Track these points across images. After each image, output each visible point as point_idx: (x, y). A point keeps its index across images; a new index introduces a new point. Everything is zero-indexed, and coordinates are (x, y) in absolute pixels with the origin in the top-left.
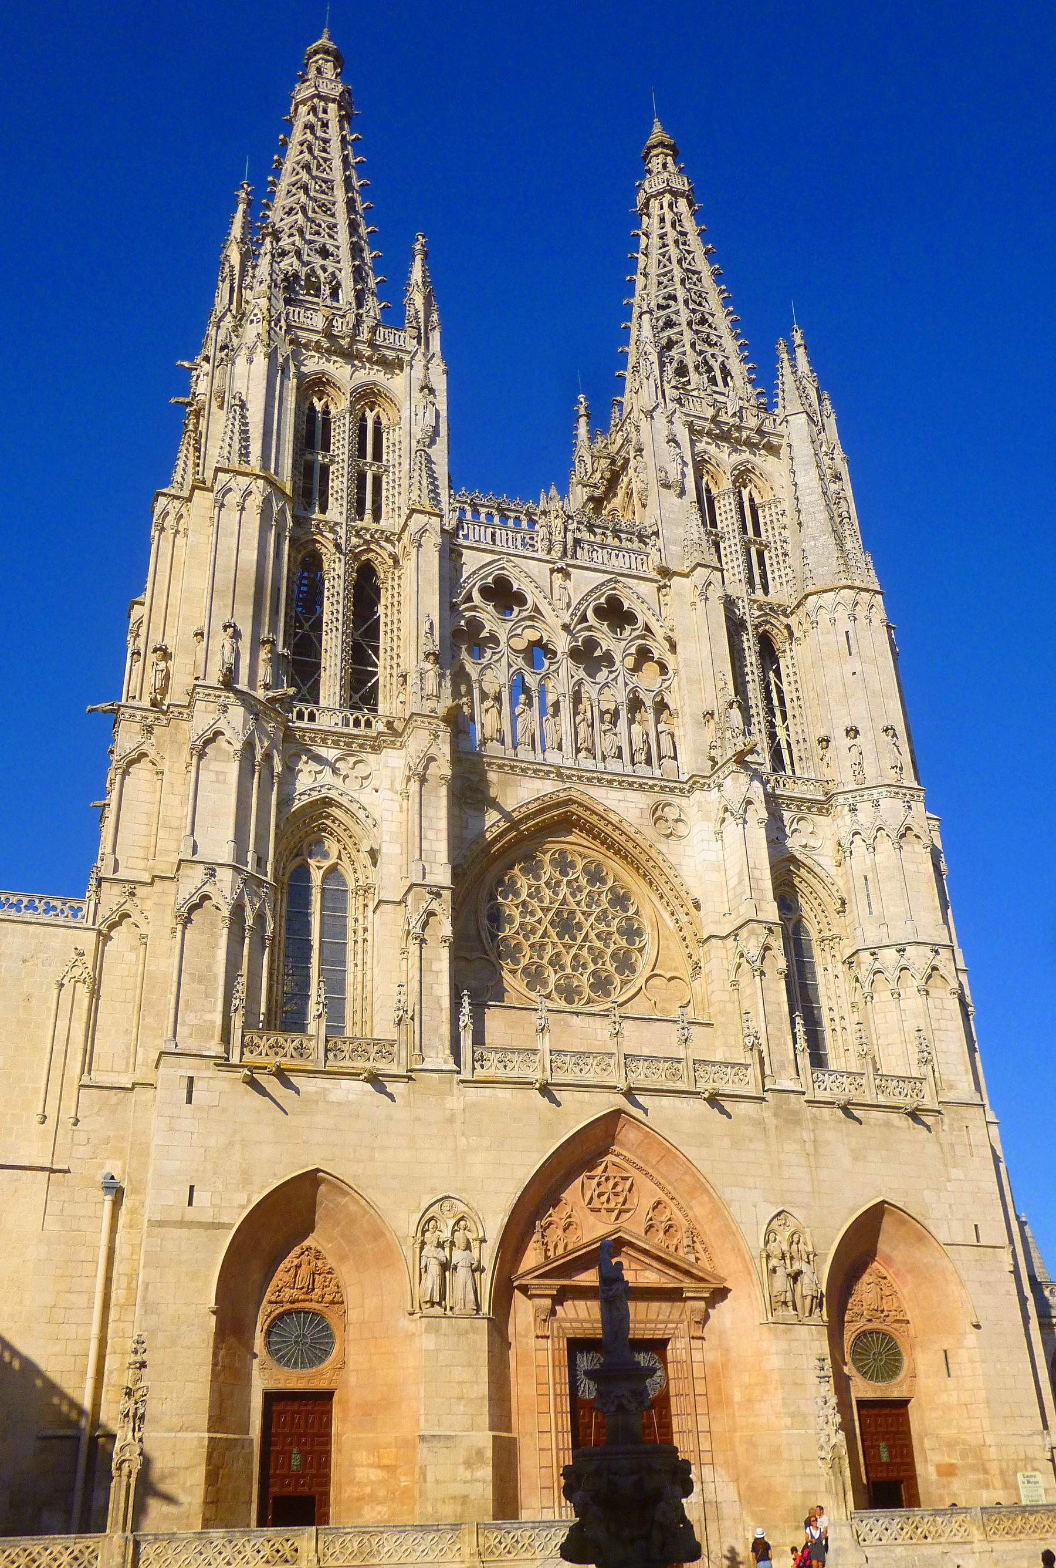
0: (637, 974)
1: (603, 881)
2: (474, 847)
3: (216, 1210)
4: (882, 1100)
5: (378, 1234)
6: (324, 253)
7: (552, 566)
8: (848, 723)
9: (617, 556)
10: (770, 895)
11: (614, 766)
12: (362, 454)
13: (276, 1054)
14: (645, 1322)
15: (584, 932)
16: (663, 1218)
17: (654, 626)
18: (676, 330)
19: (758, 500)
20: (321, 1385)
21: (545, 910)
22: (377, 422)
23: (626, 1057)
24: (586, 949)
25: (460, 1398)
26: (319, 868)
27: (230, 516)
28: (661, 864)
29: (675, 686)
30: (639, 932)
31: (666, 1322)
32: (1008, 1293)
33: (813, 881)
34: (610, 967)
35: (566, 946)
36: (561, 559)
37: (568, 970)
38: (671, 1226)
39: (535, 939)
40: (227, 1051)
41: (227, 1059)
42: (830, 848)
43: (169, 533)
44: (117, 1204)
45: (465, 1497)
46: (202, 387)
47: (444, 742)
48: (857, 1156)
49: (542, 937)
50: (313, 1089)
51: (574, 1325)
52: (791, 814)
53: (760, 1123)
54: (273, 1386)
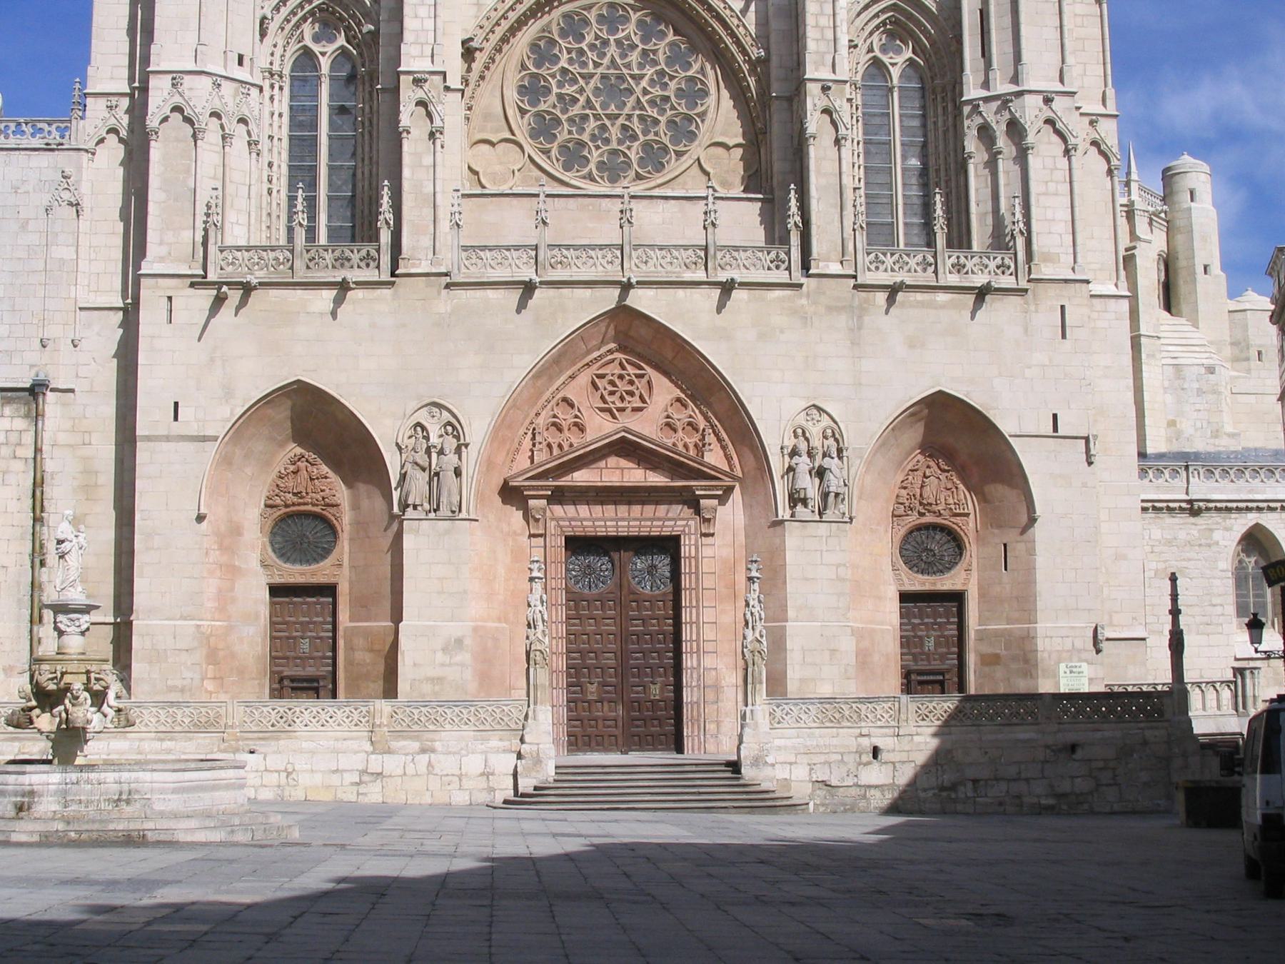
0: (696, 143)
2: (493, 14)
3: (201, 424)
4: (954, 279)
14: (652, 520)
15: (631, 101)
23: (637, 247)
24: (635, 119)
26: (323, 54)
30: (705, 93)
38: (690, 424)
39: (576, 110)
40: (205, 268)
41: (205, 277)
48: (913, 343)
49: (584, 108)
51: (573, 523)
54: (278, 580)
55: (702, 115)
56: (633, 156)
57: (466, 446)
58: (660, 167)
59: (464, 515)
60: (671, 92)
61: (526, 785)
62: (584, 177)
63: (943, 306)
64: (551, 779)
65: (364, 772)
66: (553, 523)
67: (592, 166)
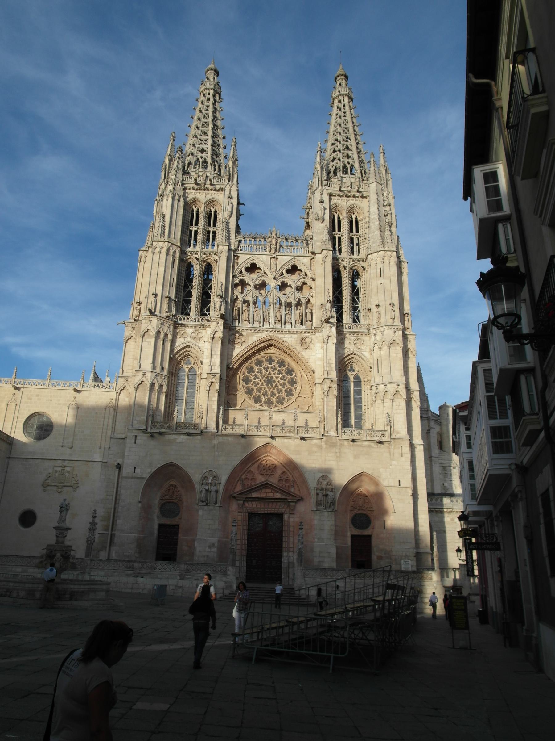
1: (284, 366)
4: (368, 438)
5: (190, 481)
6: (203, 151)
7: (271, 256)
8: (377, 303)
9: (297, 249)
10: (334, 369)
11: (288, 326)
12: (209, 225)
13: (162, 428)
16: (285, 477)
17: (308, 273)
18: (336, 153)
19: (359, 219)
20: (175, 523)
21: (262, 377)
22: (216, 212)
24: (276, 389)
25: (209, 529)
27: (156, 257)
28: (302, 359)
29: (314, 295)
30: (296, 383)
31: (282, 509)
32: (409, 503)
33: (362, 361)
34: (284, 395)
35: (269, 389)
36: (274, 253)
37: (269, 396)
38: (287, 479)
39: (258, 386)
41: (147, 430)
42: (368, 350)
43: (142, 263)
44: (119, 472)
45: (208, 556)
46: (155, 211)
47: (220, 326)
48: (356, 457)
49: (261, 386)
50: (172, 438)
52: (354, 337)
53: (320, 447)
55: (296, 389)
56: (274, 399)
57: (220, 483)
58: (282, 404)
59: (217, 505)
60: (286, 382)
61: (227, 592)
62: (260, 405)
63: (364, 447)
64: (234, 591)
65: (176, 586)
66: (245, 509)
67: (263, 402)
